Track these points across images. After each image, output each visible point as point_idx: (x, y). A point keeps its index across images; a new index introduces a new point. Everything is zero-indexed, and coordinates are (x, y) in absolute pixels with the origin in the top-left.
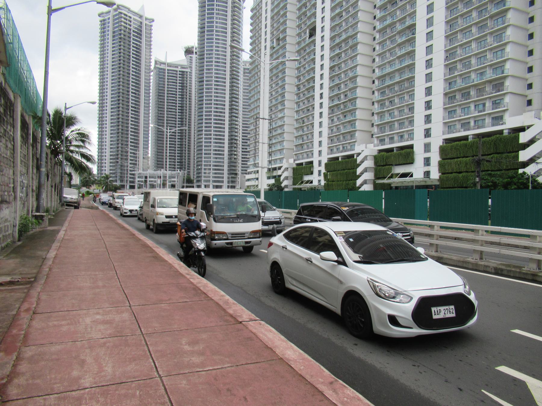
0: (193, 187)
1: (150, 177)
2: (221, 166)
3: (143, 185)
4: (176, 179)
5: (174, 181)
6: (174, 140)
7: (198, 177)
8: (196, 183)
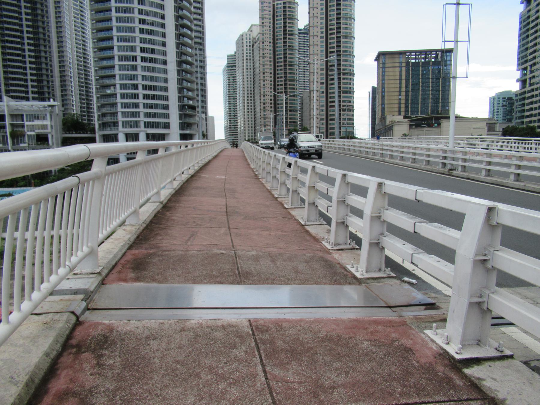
0: (92, 140)
2: (161, 89)
4: (47, 122)
5: (44, 127)
6: (19, 46)
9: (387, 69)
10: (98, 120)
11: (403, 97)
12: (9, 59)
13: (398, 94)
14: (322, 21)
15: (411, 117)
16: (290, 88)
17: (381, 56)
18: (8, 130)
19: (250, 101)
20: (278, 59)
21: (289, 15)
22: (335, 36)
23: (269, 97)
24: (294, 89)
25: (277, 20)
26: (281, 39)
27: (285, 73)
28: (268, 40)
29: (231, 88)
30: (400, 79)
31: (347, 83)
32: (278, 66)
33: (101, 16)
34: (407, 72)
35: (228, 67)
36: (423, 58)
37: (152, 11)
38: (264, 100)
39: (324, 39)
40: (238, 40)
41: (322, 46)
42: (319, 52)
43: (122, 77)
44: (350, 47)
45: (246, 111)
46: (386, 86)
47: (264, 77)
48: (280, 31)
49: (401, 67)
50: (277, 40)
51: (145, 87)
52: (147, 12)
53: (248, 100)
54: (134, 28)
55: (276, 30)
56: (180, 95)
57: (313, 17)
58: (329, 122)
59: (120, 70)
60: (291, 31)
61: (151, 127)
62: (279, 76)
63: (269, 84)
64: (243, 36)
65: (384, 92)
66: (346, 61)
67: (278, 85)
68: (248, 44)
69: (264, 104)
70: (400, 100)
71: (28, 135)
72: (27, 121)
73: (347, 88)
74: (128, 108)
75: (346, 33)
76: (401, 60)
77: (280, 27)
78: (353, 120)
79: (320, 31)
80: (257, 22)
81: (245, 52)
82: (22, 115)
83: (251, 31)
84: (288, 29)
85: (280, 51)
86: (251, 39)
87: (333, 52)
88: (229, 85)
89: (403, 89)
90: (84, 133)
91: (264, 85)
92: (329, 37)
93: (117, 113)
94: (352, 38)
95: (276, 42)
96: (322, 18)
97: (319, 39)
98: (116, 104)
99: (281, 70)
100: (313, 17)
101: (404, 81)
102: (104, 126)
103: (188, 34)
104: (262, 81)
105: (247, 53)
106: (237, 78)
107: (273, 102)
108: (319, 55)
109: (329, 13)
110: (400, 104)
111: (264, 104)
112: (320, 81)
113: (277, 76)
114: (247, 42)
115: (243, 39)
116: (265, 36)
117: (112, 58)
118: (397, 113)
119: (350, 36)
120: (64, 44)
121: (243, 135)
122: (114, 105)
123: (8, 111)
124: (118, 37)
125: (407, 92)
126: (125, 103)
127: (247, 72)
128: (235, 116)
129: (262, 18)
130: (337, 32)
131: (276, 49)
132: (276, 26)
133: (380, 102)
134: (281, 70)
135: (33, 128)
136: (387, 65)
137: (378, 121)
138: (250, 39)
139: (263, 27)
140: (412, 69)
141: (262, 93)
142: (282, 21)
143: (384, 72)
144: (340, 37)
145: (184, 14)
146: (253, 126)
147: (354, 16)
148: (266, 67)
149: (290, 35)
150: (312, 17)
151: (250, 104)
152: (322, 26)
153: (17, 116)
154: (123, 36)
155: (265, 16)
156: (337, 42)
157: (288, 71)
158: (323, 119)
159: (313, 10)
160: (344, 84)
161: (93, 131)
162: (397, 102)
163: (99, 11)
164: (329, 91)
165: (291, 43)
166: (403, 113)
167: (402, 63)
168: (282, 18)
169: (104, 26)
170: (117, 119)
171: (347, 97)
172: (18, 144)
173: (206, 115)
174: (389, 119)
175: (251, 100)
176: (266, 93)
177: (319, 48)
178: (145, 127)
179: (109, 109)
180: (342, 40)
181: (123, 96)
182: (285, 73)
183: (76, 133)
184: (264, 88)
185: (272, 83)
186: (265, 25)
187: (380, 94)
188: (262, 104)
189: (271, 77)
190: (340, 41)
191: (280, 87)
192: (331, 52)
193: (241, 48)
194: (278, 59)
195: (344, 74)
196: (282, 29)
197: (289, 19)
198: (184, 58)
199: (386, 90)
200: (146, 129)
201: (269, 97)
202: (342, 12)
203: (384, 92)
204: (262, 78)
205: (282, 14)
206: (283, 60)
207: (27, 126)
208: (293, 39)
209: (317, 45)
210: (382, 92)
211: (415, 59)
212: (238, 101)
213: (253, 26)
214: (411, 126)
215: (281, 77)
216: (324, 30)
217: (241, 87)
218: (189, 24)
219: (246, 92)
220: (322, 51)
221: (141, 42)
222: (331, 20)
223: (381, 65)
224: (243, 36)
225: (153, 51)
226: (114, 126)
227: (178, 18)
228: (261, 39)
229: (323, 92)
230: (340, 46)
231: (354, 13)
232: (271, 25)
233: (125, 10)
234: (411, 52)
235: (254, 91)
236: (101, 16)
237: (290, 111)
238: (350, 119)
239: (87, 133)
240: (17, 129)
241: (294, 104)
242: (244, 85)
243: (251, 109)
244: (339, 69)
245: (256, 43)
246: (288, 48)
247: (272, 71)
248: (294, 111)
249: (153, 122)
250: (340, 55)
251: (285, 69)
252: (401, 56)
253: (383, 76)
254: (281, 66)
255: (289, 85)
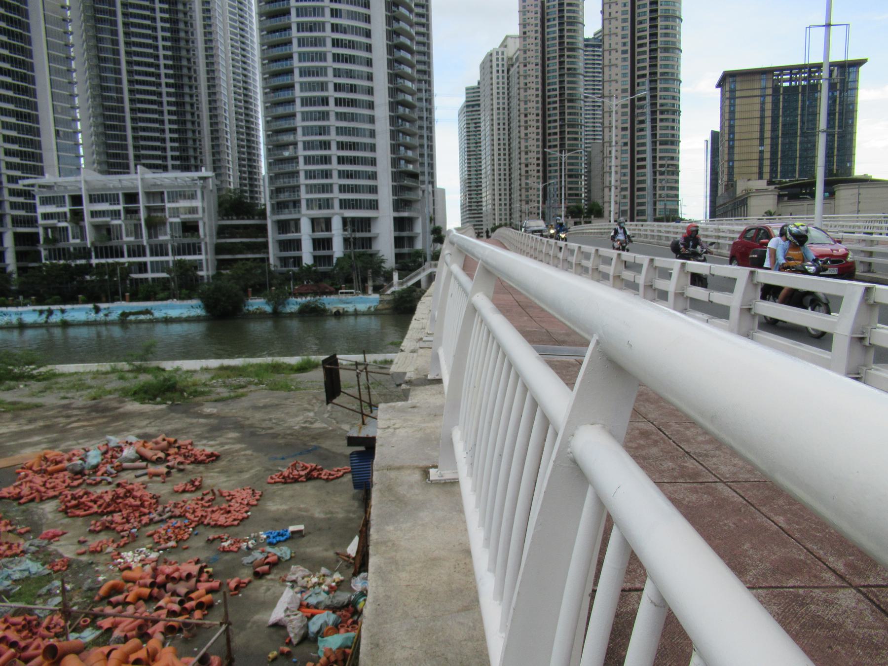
1: (93, 199)
3: (65, 229)
4: (197, 203)
5: (193, 210)
7: (278, 191)
8: (273, 212)
9: (738, 101)
10: (271, 198)
11: (767, 148)
12: (139, 109)
13: (757, 142)
14: (624, 24)
15: (780, 183)
16: (569, 139)
17: (728, 80)
18: (143, 215)
19: (502, 162)
20: (549, 91)
21: (569, 17)
22: (647, 49)
23: (535, 155)
24: (576, 139)
25: (548, 27)
26: (554, 58)
27: (562, 113)
28: (533, 60)
29: (472, 141)
30: (762, 118)
31: (667, 128)
32: (549, 103)
33: (276, 37)
34: (775, 104)
35: (467, 106)
36: (804, 79)
37: (352, 26)
38: (526, 159)
39: (628, 55)
40: (483, 62)
41: (624, 67)
42: (619, 77)
43: (307, 131)
44: (673, 67)
45: (496, 177)
46: (737, 129)
47: (526, 122)
48: (554, 45)
49: (763, 96)
50: (549, 59)
51: (341, 146)
52: (345, 28)
53: (499, 160)
54: (325, 54)
55: (547, 43)
56: (394, 156)
57: (610, 20)
58: (636, 193)
59: (303, 120)
60: (572, 43)
61: (349, 208)
62: (551, 119)
63: (534, 132)
64: (491, 55)
65: (731, 140)
66: (666, 90)
67: (550, 134)
68: (500, 69)
69: (527, 166)
70: (761, 152)
71: (171, 223)
72: (169, 202)
73: (666, 135)
74: (315, 178)
75: (667, 42)
76: (763, 84)
77: (554, 39)
78: (677, 189)
79: (619, 39)
80: (515, 30)
81: (495, 81)
82: (162, 193)
83: (506, 46)
84: (566, 40)
85: (554, 78)
86: (505, 57)
87: (644, 76)
88: (468, 136)
89: (768, 134)
90: (249, 219)
91: (526, 135)
92: (637, 50)
93: (299, 186)
94: (677, 51)
95: (547, 62)
96: (624, 21)
97: (619, 55)
98: (298, 172)
99: (555, 108)
100: (610, 20)
101: (768, 121)
102: (279, 206)
103: (408, 60)
104: (522, 129)
105: (498, 83)
106: (482, 125)
107: (540, 162)
108: (620, 82)
109: (637, 11)
110: (761, 160)
111: (527, 166)
112: (620, 126)
113: (548, 119)
114: (498, 65)
115: (491, 61)
116: (529, 54)
117: (292, 102)
118: (757, 176)
119: (673, 48)
120: (217, 82)
121: (490, 218)
122: (295, 174)
123: (143, 187)
124: (300, 68)
125: (774, 139)
126: (310, 171)
127: (499, 114)
128: (477, 186)
129: (523, 25)
130: (651, 43)
131: (547, 75)
132: (547, 37)
133: (726, 158)
134: (555, 108)
135: (178, 212)
136: (738, 94)
137: (721, 190)
138: (503, 59)
139: (525, 39)
140: (784, 98)
141: (523, 148)
142: (557, 28)
143: (732, 105)
144: (656, 50)
145: (401, 29)
146: (508, 202)
147: (680, 12)
148: (530, 105)
149: (569, 50)
150: (607, 17)
151: (502, 167)
152: (624, 32)
153: (155, 195)
154: (309, 68)
155: (528, 21)
156: (650, 58)
157: (567, 111)
158: (625, 189)
159: (610, 7)
160: (662, 128)
161: (263, 214)
162: (756, 156)
163: (272, 31)
164: (637, 141)
165: (573, 63)
166: (767, 176)
167: (765, 88)
168: (557, 22)
169: (280, 53)
170: (299, 196)
171: (667, 151)
172: (156, 236)
173: (433, 187)
174: (741, 187)
175: (505, 160)
176: (529, 148)
177: (619, 70)
178: (341, 208)
179: (286, 180)
180: (659, 55)
181: (308, 160)
182: (562, 113)
183: (238, 219)
184: (526, 140)
185: (540, 131)
186: (529, 37)
187: (726, 144)
188: (523, 166)
189: (538, 121)
190: (656, 58)
191: (552, 137)
192: (640, 77)
193: (489, 76)
194: (549, 91)
195: (662, 113)
196: (557, 41)
197: (569, 24)
198: (401, 97)
199: (737, 137)
200: (342, 211)
201: (535, 155)
202: (659, 8)
203: (733, 140)
204: (522, 123)
205: (557, 15)
206: (557, 93)
207: (169, 208)
208: (574, 57)
209: (616, 66)
210: (730, 140)
211: (790, 80)
212: (483, 162)
213: (509, 39)
214: (780, 197)
215: (555, 121)
216: (628, 40)
217: (488, 138)
218: (408, 42)
219: (496, 147)
220: (624, 75)
221: (335, 76)
222: (640, 23)
223: (727, 95)
224: (491, 55)
225: (353, 89)
226: (295, 207)
227: (392, 34)
228: (521, 60)
229: (625, 144)
230: (656, 65)
231: (680, 8)
232: (539, 35)
233: (311, 27)
234: (781, 70)
235: (509, 145)
236: (276, 37)
237: (570, 176)
238: (672, 188)
239: (253, 219)
240: (155, 214)
241: (577, 164)
242: (493, 135)
243: (505, 175)
244: (654, 105)
245: (512, 65)
246: (567, 72)
247: (540, 112)
248: (576, 176)
249: (353, 200)
250: (656, 81)
251: (562, 107)
252: (764, 76)
253: (732, 113)
254: (555, 102)
255: (569, 133)
